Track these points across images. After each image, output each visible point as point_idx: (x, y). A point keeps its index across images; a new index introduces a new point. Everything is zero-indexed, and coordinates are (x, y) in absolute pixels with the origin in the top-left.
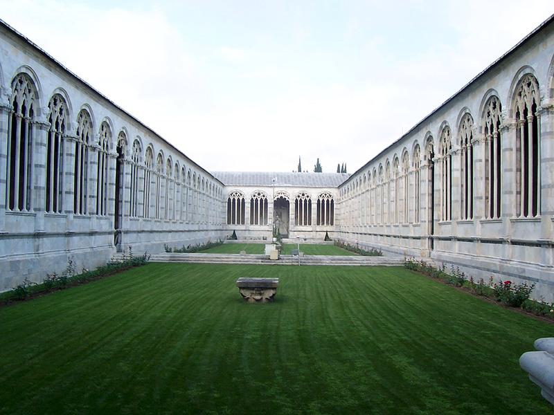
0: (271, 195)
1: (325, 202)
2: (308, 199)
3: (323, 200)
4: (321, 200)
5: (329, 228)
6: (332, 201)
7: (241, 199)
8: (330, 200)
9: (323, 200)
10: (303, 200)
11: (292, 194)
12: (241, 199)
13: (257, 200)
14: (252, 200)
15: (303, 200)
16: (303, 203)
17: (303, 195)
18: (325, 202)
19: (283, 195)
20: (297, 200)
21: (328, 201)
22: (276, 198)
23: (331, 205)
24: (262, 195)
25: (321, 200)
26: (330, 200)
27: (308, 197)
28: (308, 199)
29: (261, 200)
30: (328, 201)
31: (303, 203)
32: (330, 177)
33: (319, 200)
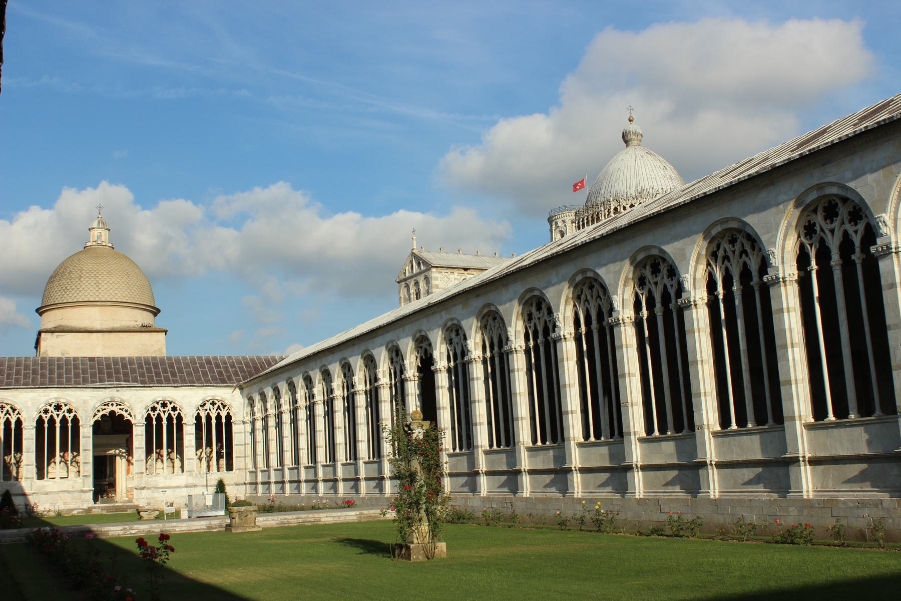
0: (87, 403)
1: (214, 422)
2: (174, 415)
3: (209, 417)
4: (203, 415)
5: (225, 475)
6: (229, 417)
7: (13, 421)
8: (223, 414)
9: (209, 417)
10: (164, 417)
11: (137, 402)
12: (13, 421)
13: (52, 421)
14: (40, 421)
15: (164, 417)
16: (165, 423)
17: (164, 405)
18: (214, 422)
19: (116, 409)
20: (149, 419)
21: (219, 417)
22: (99, 415)
23: (225, 427)
24: (65, 408)
25: (203, 415)
26: (223, 414)
27: (174, 409)
28: (174, 415)
29: (64, 420)
30: (219, 417)
31: (165, 423)
32: (218, 366)
33: (198, 418)
